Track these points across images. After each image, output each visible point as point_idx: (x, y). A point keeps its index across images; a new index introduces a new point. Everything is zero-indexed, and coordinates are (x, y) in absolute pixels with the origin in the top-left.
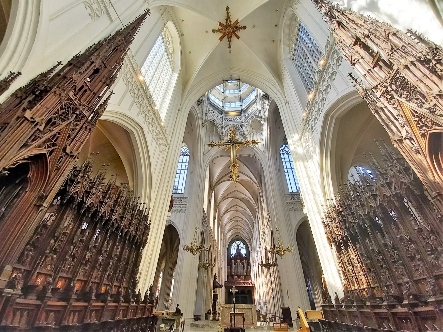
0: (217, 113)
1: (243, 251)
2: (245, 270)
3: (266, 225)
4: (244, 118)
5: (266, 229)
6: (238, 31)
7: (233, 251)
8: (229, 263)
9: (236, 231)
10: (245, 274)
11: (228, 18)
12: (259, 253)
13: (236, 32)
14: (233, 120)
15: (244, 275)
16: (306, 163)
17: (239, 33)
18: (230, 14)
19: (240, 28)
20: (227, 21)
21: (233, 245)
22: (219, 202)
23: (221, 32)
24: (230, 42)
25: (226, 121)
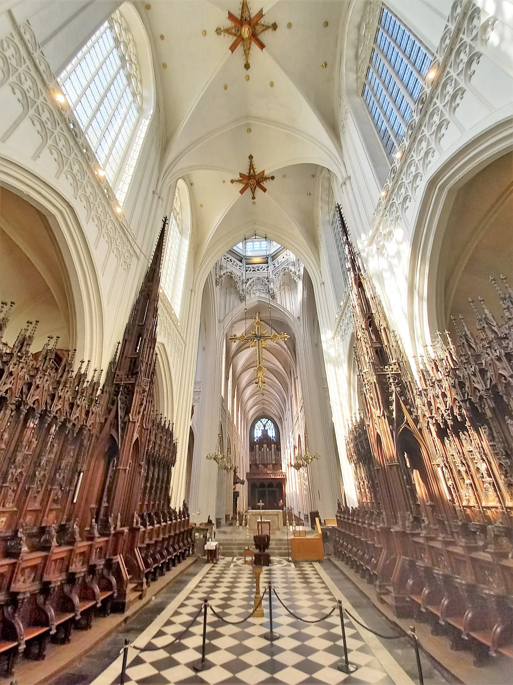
0: (235, 260)
1: (271, 433)
2: (273, 457)
3: (299, 409)
4: (271, 268)
5: (299, 414)
6: (264, 182)
7: (258, 434)
8: (252, 448)
9: (261, 406)
10: (274, 462)
11: (251, 167)
12: (291, 440)
13: (262, 184)
14: (258, 270)
15: (272, 464)
16: (337, 369)
17: (265, 184)
18: (253, 163)
19: (266, 179)
20: (250, 171)
21: (258, 424)
22: (238, 374)
23: (243, 183)
24: (253, 193)
25: (248, 272)
